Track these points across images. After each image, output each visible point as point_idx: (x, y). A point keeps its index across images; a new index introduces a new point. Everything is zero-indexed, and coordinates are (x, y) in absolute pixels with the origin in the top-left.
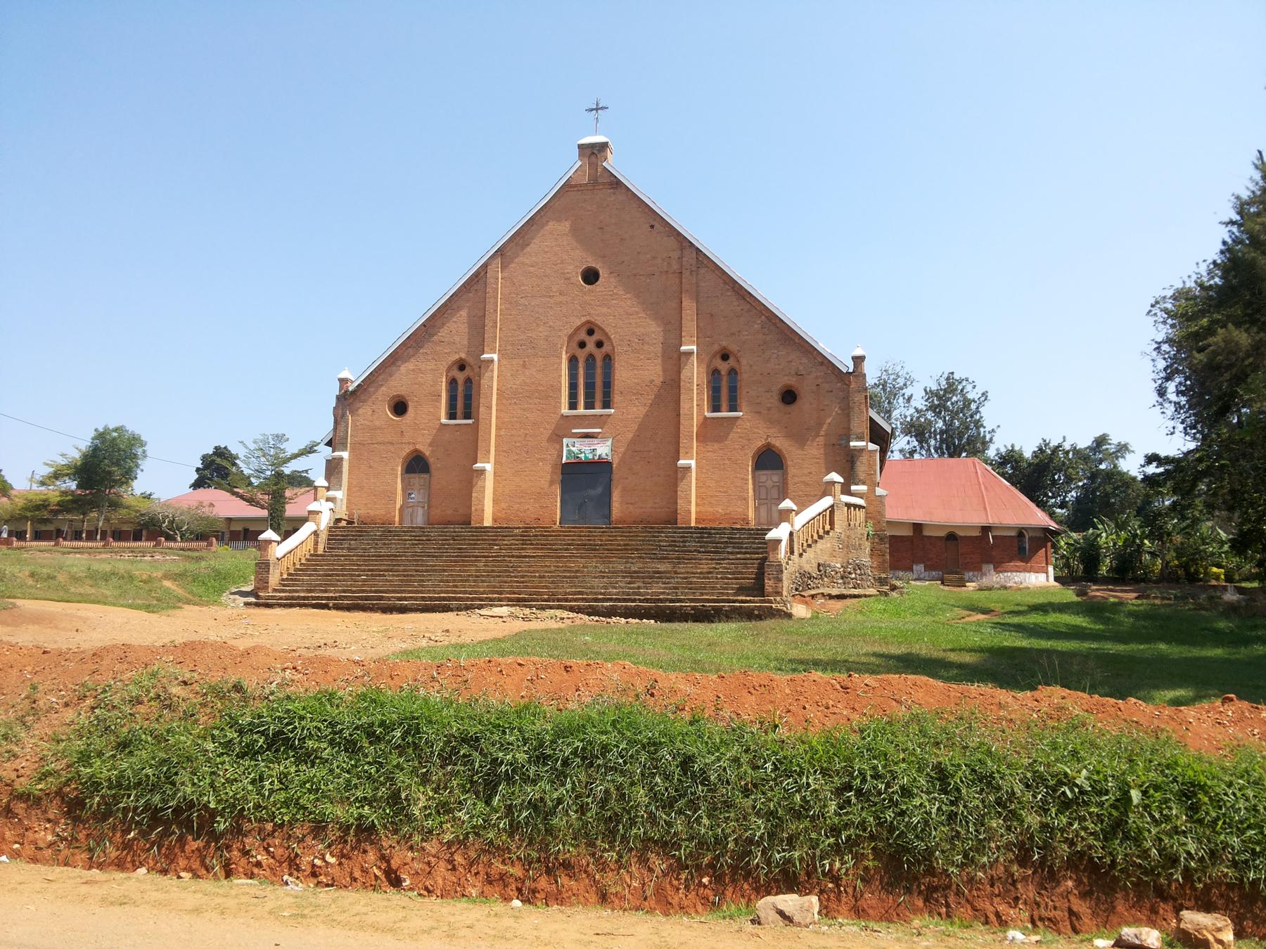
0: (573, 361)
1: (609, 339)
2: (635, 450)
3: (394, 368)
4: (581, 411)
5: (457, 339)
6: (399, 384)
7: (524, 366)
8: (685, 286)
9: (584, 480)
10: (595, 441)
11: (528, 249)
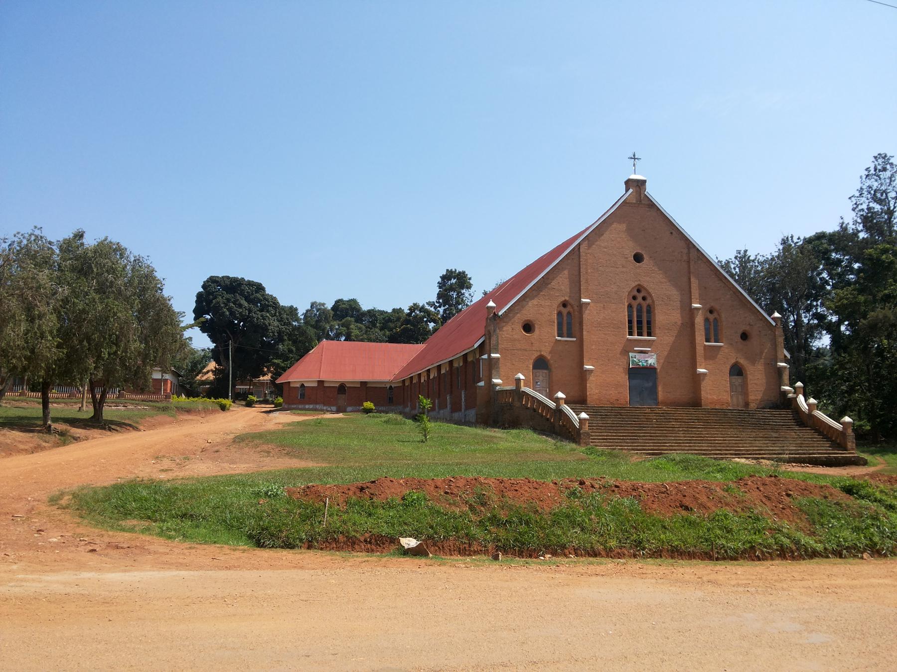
0: (630, 306)
1: (651, 296)
2: (668, 361)
3: (524, 303)
4: (636, 337)
5: (563, 287)
6: (529, 312)
7: (604, 308)
8: (692, 270)
9: (641, 376)
10: (647, 355)
11: (602, 238)
